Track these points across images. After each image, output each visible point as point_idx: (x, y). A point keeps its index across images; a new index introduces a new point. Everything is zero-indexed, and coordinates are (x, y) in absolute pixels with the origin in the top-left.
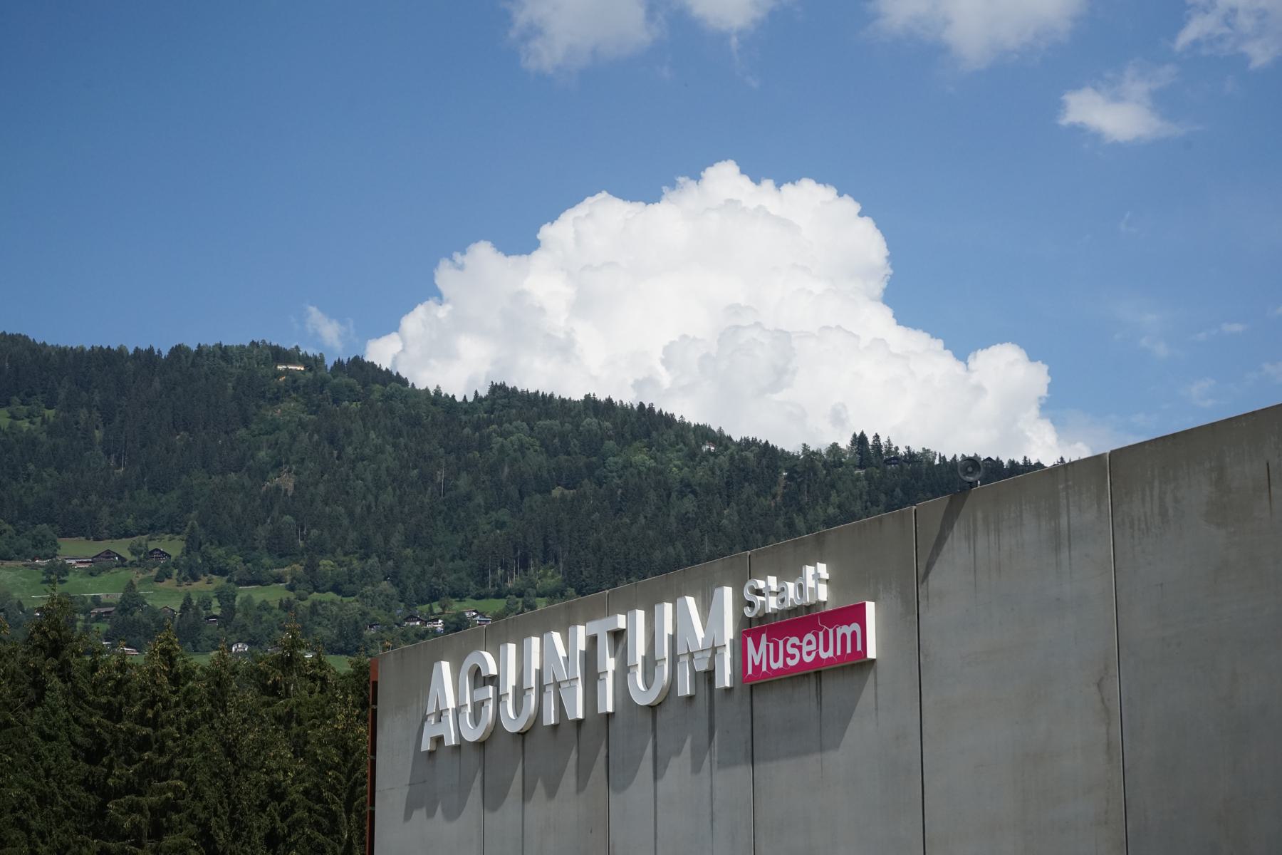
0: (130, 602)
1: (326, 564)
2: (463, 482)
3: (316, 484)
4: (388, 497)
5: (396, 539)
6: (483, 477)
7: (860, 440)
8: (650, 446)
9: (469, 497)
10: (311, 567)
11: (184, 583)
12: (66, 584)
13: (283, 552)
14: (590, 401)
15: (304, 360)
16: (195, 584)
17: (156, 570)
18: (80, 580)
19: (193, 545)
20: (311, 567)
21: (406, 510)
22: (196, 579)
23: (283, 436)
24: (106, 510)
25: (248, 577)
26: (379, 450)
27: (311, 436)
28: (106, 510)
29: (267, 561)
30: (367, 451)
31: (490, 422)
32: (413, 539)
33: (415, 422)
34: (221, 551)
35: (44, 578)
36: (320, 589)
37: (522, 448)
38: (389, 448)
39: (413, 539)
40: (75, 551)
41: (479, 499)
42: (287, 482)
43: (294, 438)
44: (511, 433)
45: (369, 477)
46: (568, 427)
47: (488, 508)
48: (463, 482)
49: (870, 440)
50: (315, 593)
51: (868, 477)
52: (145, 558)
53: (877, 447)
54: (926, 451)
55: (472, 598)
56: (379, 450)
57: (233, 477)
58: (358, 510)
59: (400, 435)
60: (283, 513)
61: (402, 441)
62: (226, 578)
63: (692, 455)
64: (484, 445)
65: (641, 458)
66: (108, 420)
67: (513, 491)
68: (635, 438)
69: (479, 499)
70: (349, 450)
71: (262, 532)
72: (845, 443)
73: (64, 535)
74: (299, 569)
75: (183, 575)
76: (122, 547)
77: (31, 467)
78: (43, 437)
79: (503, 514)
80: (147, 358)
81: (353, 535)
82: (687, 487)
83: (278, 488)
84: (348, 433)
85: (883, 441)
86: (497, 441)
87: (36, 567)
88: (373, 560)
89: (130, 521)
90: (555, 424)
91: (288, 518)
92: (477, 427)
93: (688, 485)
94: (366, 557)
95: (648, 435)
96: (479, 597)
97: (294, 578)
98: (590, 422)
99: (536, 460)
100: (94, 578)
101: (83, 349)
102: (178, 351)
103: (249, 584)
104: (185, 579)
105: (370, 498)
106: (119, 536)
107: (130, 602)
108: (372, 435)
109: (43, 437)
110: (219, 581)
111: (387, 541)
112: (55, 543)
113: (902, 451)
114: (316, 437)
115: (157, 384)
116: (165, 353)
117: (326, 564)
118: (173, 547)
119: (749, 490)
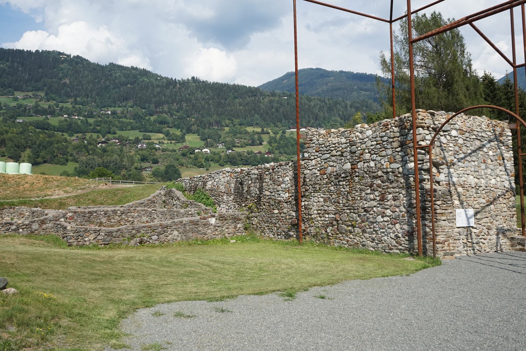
1: (78, 99)
2: (108, 83)
3: (74, 82)
4: (91, 85)
5: (94, 94)
6: (112, 82)
7: (193, 78)
8: (147, 77)
9: (110, 86)
10: (76, 100)
13: (69, 96)
14: (132, 67)
15: (66, 55)
17: (39, 99)
19: (47, 94)
20: (76, 100)
21: (96, 88)
22: (49, 101)
23: (65, 71)
24: (24, 86)
26: (88, 75)
27: (72, 71)
28: (24, 86)
29: (65, 98)
30: (85, 75)
31: (111, 71)
32: (97, 95)
33: (95, 69)
34: (54, 95)
37: (120, 76)
38: (90, 75)
39: (97, 95)
40: (19, 95)
41: (112, 87)
42: (67, 81)
43: (68, 72)
44: (117, 73)
45: (86, 80)
46: (129, 72)
47: (113, 89)
48: (108, 83)
49: (195, 78)
51: (196, 85)
52: (36, 96)
53: (197, 79)
54: (206, 81)
56: (88, 75)
57: (54, 80)
58: (85, 88)
59: (92, 72)
60: (67, 88)
61: (92, 73)
63: (157, 80)
64: (111, 75)
65: (146, 79)
66: (22, 66)
67: (119, 85)
68: (144, 75)
69: (112, 87)
70: (81, 75)
71: (63, 91)
72: (190, 78)
73: (15, 91)
74: (73, 100)
76: (30, 94)
77: (5, 75)
78: (7, 69)
79: (117, 90)
80: (29, 53)
81: (84, 93)
82: (158, 86)
83: (65, 82)
84: (80, 71)
85: (198, 78)
86: (114, 75)
87: (10, 97)
88: (89, 99)
89: (30, 88)
90: (126, 71)
91: (69, 89)
92: (109, 71)
93: (158, 85)
94: (87, 98)
95: (146, 75)
96: (115, 107)
98: (133, 71)
99: (123, 79)
101: (14, 49)
102: (37, 51)
103: (61, 103)
105: (87, 85)
106: (28, 91)
108: (86, 72)
109: (7, 69)
110: (55, 102)
111: (92, 95)
112: (13, 93)
113: (202, 80)
114: (73, 72)
115: (33, 58)
116: (34, 52)
117: (78, 99)
118: (42, 94)
119: (171, 87)
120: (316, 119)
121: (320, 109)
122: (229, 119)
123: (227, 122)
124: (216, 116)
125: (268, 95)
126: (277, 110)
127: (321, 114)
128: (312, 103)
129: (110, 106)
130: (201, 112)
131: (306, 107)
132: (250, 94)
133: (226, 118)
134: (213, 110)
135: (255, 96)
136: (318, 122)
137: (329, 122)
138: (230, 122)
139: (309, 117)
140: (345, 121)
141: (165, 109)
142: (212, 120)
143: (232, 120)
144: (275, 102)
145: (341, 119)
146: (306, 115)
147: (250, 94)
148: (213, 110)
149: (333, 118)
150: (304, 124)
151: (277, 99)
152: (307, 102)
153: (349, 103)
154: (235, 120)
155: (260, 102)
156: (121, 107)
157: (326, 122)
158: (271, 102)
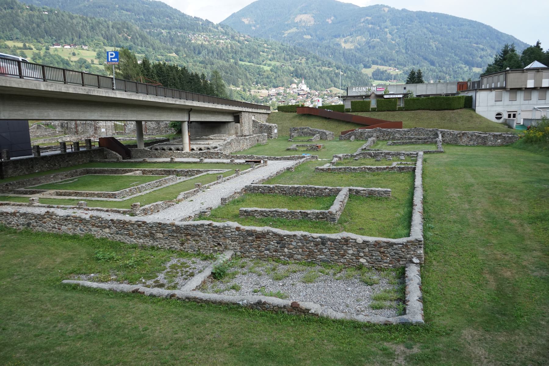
120: (80, 37)
121: (83, 27)
125: (27, 9)
126: (38, 26)
127: (84, 33)
128: (75, 21)
131: (69, 24)
132: (6, 6)
135: (12, 8)
136: (81, 40)
137: (92, 41)
139: (72, 35)
140: (107, 40)
144: (36, 17)
145: (104, 38)
146: (70, 33)
147: (6, 6)
149: (96, 37)
150: (68, 41)
151: (37, 13)
152: (69, 20)
153: (111, 23)
155: (18, 16)
157: (89, 40)
158: (31, 16)
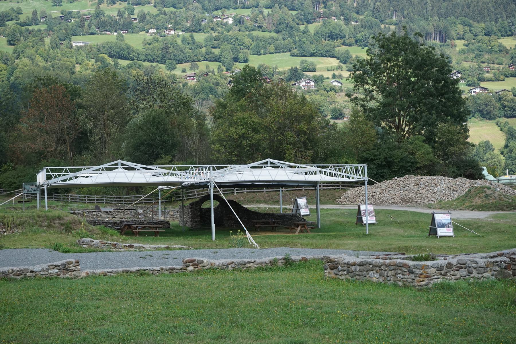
0: (99, 14)
11: (110, 5)
12: (62, 7)
16: (114, 5)
18: (67, 5)
22: (114, 3)
25: (136, 2)
35: (52, 4)
36: (167, 6)
50: (165, 8)
55: (233, 9)
62: (126, 3)
75: (109, 2)
97: (155, 2)
100: (72, 4)
103: (137, 5)
104: (110, 3)
107: (99, 14)
122: (464, 24)
123: (461, 29)
124: (436, 18)
129: (228, 8)
130: (406, 12)
133: (458, 22)
134: (429, 8)
138: (467, 28)
141: (334, 9)
142: (430, 28)
143: (470, 26)
148: (429, 8)
154: (476, 24)
156: (248, 8)
